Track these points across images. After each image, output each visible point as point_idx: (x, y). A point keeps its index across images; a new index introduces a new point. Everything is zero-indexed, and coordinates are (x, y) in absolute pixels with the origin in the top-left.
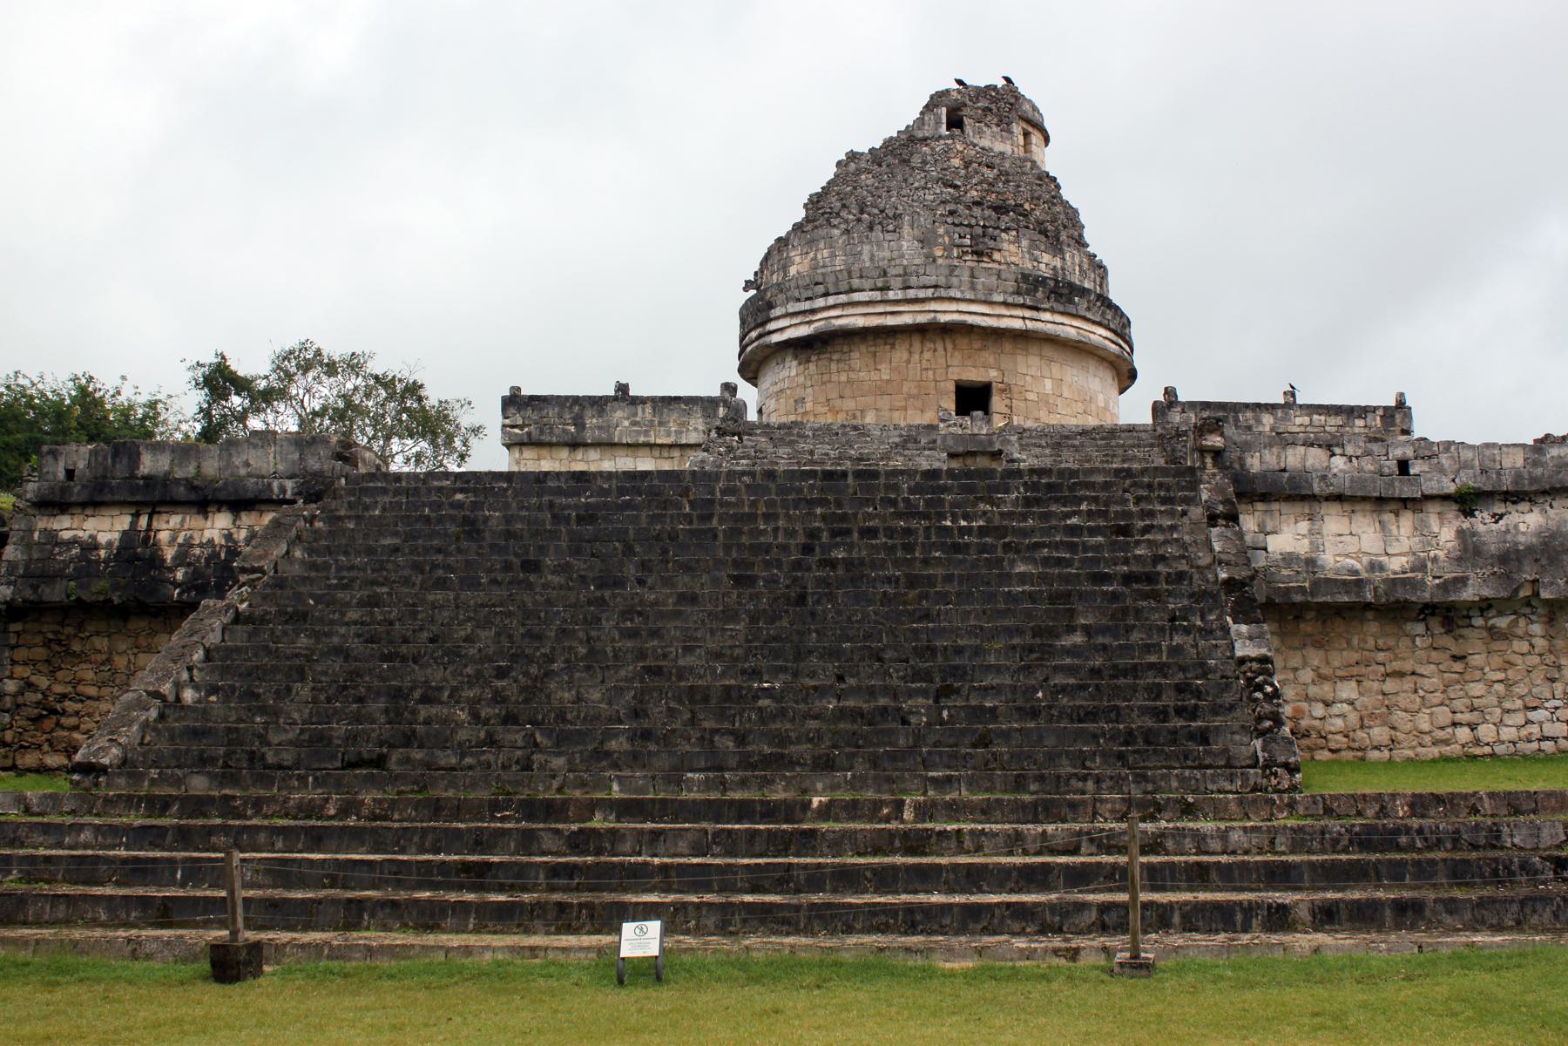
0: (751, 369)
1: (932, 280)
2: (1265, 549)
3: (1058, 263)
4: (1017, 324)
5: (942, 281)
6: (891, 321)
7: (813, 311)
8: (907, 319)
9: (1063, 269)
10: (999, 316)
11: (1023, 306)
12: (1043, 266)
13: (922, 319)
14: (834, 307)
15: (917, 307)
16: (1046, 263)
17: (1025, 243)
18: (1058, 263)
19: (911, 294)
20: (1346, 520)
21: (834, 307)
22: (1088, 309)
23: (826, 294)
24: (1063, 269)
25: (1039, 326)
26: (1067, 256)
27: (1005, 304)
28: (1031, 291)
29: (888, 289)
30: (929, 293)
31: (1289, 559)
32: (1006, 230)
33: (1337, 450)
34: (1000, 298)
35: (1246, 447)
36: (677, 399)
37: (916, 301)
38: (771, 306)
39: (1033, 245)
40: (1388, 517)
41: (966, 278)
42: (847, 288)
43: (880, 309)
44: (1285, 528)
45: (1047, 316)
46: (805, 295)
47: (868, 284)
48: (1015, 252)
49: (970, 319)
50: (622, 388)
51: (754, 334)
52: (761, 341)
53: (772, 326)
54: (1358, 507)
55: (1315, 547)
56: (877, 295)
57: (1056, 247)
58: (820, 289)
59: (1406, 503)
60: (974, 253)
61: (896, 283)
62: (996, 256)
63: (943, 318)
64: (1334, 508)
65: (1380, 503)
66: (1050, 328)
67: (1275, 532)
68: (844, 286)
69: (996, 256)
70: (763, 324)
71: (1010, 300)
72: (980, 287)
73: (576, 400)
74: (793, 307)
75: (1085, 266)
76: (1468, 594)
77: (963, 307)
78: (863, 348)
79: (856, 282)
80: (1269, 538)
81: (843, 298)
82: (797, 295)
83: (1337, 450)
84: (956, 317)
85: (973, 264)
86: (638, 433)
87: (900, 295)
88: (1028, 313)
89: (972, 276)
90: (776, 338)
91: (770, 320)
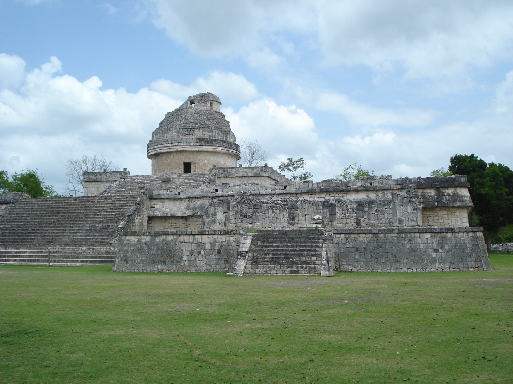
3: (211, 134)
4: (196, 149)
6: (169, 151)
8: (172, 150)
13: (175, 150)
16: (206, 135)
17: (201, 131)
19: (173, 144)
30: (176, 144)
31: (158, 209)
35: (154, 190)
39: (204, 131)
41: (185, 141)
45: (205, 147)
48: (198, 133)
49: (185, 149)
55: (162, 207)
61: (170, 142)
63: (179, 150)
64: (167, 200)
76: (185, 215)
79: (162, 143)
84: (182, 149)
88: (199, 147)
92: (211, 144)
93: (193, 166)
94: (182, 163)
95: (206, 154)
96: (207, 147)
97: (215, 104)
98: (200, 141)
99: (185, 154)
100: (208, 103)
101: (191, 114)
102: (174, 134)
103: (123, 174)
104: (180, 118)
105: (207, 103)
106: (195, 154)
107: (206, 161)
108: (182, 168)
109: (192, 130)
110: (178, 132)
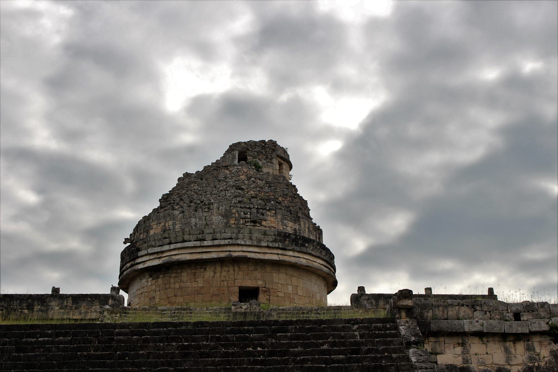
0: (125, 282)
1: (228, 235)
2: (436, 363)
4: (275, 257)
5: (234, 236)
6: (205, 256)
7: (162, 252)
8: (214, 255)
9: (299, 230)
10: (264, 253)
11: (277, 248)
12: (289, 228)
13: (222, 255)
14: (174, 249)
15: (220, 249)
16: (290, 227)
17: (279, 217)
18: (297, 227)
19: (216, 242)
20: (484, 346)
21: (174, 249)
22: (313, 250)
23: (170, 243)
24: (299, 230)
25: (286, 259)
26: (302, 223)
27: (268, 247)
28: (283, 241)
29: (204, 240)
30: (226, 242)
32: (269, 210)
33: (478, 308)
34: (264, 244)
36: (87, 295)
37: (219, 246)
38: (139, 250)
40: (509, 344)
42: (181, 240)
43: (200, 250)
44: (447, 350)
45: (291, 253)
46: (158, 244)
47: (192, 238)
50: (56, 290)
51: (128, 265)
52: (133, 268)
53: (139, 260)
54: (490, 339)
55: (466, 361)
56: (198, 243)
57: (297, 220)
58: (167, 241)
59: (517, 337)
60: (251, 222)
61: (210, 237)
62: (264, 223)
64: (476, 340)
65: (504, 337)
66: (293, 260)
67: (442, 353)
68: (180, 239)
69: (264, 223)
70: (134, 259)
71: (271, 245)
72: (254, 238)
73: (30, 296)
74: (150, 251)
75: (311, 229)
77: (245, 249)
78: (189, 271)
79: (186, 237)
80: (439, 357)
81: (179, 245)
82: (153, 243)
83: (478, 308)
85: (251, 227)
86: (64, 313)
87: (210, 243)
88: (280, 252)
89: (251, 233)
90: (141, 266)
91: (138, 257)
92: (304, 249)
93: (262, 298)
94: (237, 290)
95: (290, 271)
96: (297, 254)
97: (285, 166)
98: (282, 237)
99: (244, 267)
100: (275, 161)
101: (249, 178)
102: (216, 219)
103: (110, 302)
104: (222, 186)
105: (275, 161)
106: (268, 269)
107: (290, 288)
108: (235, 298)
109: (261, 210)
110: (227, 215)
